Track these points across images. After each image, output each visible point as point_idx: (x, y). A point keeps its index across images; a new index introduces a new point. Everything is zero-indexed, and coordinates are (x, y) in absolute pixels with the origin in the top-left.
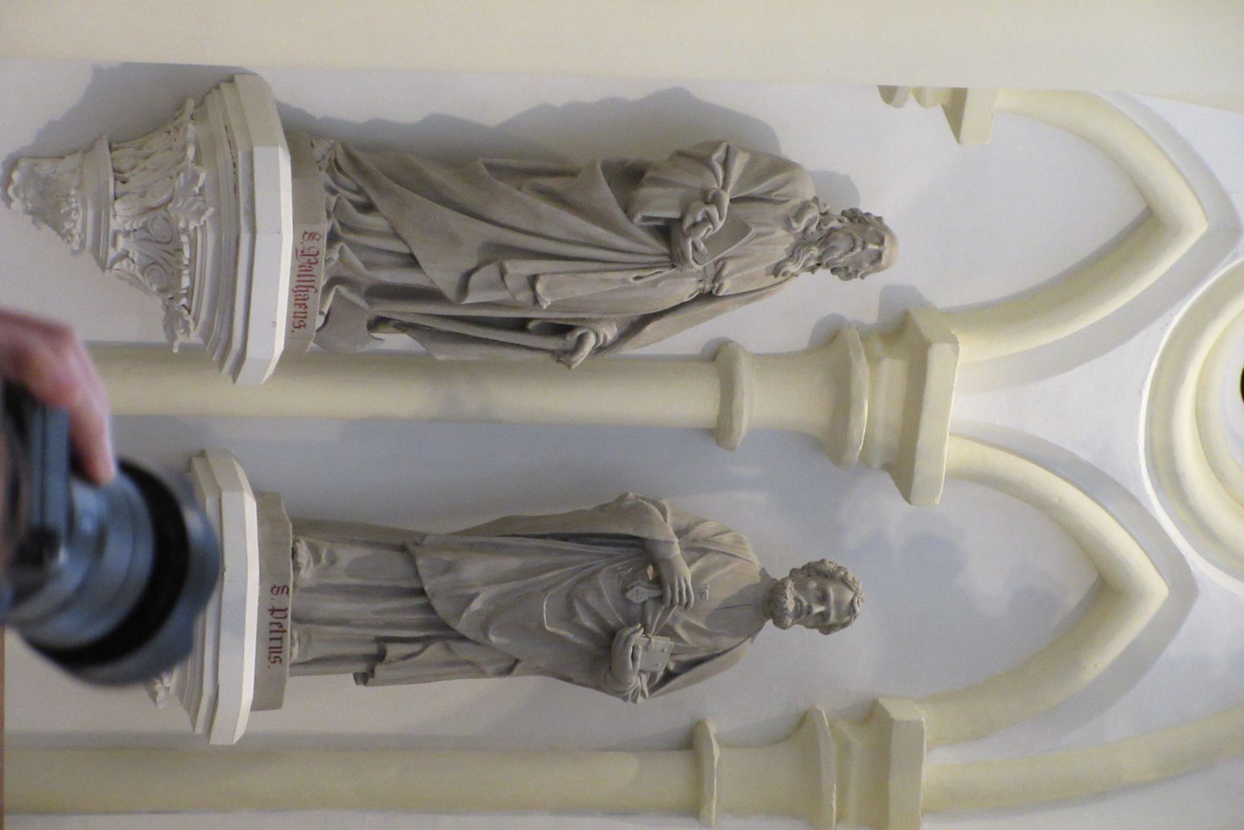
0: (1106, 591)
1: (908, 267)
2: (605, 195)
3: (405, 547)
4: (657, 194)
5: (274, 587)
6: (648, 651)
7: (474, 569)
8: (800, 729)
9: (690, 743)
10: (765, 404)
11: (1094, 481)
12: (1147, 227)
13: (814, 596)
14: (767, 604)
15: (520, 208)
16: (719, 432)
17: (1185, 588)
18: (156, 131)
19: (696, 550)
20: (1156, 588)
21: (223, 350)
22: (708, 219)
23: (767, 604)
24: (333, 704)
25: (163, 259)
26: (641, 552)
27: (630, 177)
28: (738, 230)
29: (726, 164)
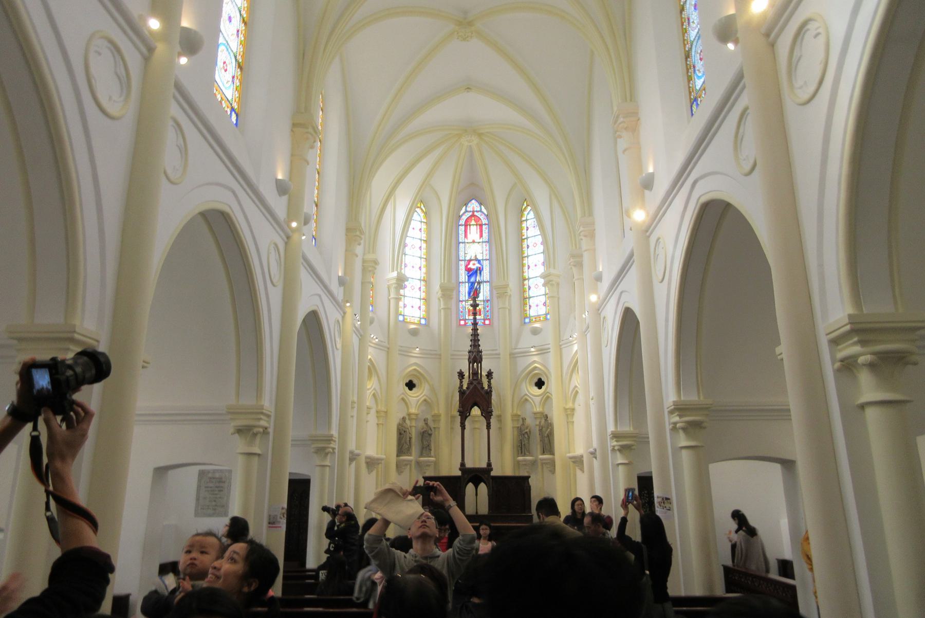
0: (425, 400)
3: (423, 448)
8: (434, 421)
10: (414, 424)
12: (403, 399)
13: (426, 420)
14: (426, 424)
18: (398, 466)
21: (411, 461)
23: (426, 424)
24: (432, 453)
25: (406, 465)
27: (400, 434)
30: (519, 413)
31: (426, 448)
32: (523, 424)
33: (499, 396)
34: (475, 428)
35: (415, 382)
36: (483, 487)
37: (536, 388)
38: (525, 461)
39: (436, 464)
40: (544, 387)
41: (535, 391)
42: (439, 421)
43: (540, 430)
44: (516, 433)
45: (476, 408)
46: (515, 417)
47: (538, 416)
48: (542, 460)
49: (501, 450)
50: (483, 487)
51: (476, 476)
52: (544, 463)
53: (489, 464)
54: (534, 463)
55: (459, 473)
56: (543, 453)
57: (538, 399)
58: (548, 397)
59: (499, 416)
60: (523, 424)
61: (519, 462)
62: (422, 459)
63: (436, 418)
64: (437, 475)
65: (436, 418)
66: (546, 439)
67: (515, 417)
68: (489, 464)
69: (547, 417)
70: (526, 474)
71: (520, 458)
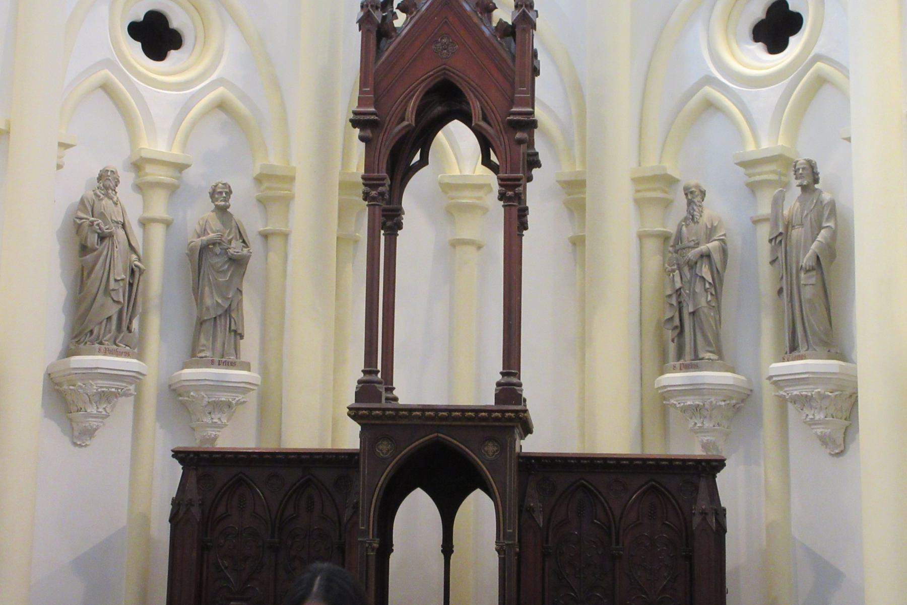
0: (222, 106)
1: (117, 163)
2: (89, 257)
3: (201, 323)
4: (90, 241)
5: (212, 364)
6: (236, 248)
7: (208, 301)
8: (263, 202)
9: (265, 236)
10: (159, 207)
11: (186, 108)
12: (106, 87)
13: (220, 195)
14: (222, 211)
15: (94, 283)
16: (168, 224)
17: (221, 81)
18: (65, 399)
19: (205, 232)
20: (220, 90)
21: (136, 379)
22: (98, 225)
23: (222, 211)
24: (250, 347)
25: (106, 397)
26: (204, 250)
27: (84, 249)
28: (102, 215)
29: (81, 219)
30: (672, 169)
31: (215, 327)
32: (691, 218)
33: (576, 90)
34: (456, 243)
35: (177, 21)
36: (479, 511)
37: (759, 49)
38: (695, 389)
39: (269, 405)
40: (796, 43)
41: (757, 60)
42: (287, 201)
43: (779, 240)
44: (654, 263)
45: (456, 127)
46: (655, 187)
47: (766, 173)
48: (778, 383)
49: (582, 343)
50: (479, 511)
51: (442, 453)
52: (794, 398)
53: (509, 391)
54: (741, 404)
55: (350, 437)
56: (793, 349)
57: (770, 95)
58: (821, 81)
59: (574, 191)
60: (691, 218)
61: (665, 395)
62: (191, 373)
63: (273, 188)
64: (269, 445)
65: (273, 188)
66: (808, 283)
67: (655, 187)
68: (509, 391)
69: (810, 176)
70: (696, 451)
71: (674, 378)
